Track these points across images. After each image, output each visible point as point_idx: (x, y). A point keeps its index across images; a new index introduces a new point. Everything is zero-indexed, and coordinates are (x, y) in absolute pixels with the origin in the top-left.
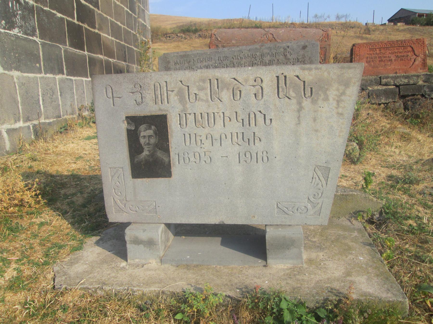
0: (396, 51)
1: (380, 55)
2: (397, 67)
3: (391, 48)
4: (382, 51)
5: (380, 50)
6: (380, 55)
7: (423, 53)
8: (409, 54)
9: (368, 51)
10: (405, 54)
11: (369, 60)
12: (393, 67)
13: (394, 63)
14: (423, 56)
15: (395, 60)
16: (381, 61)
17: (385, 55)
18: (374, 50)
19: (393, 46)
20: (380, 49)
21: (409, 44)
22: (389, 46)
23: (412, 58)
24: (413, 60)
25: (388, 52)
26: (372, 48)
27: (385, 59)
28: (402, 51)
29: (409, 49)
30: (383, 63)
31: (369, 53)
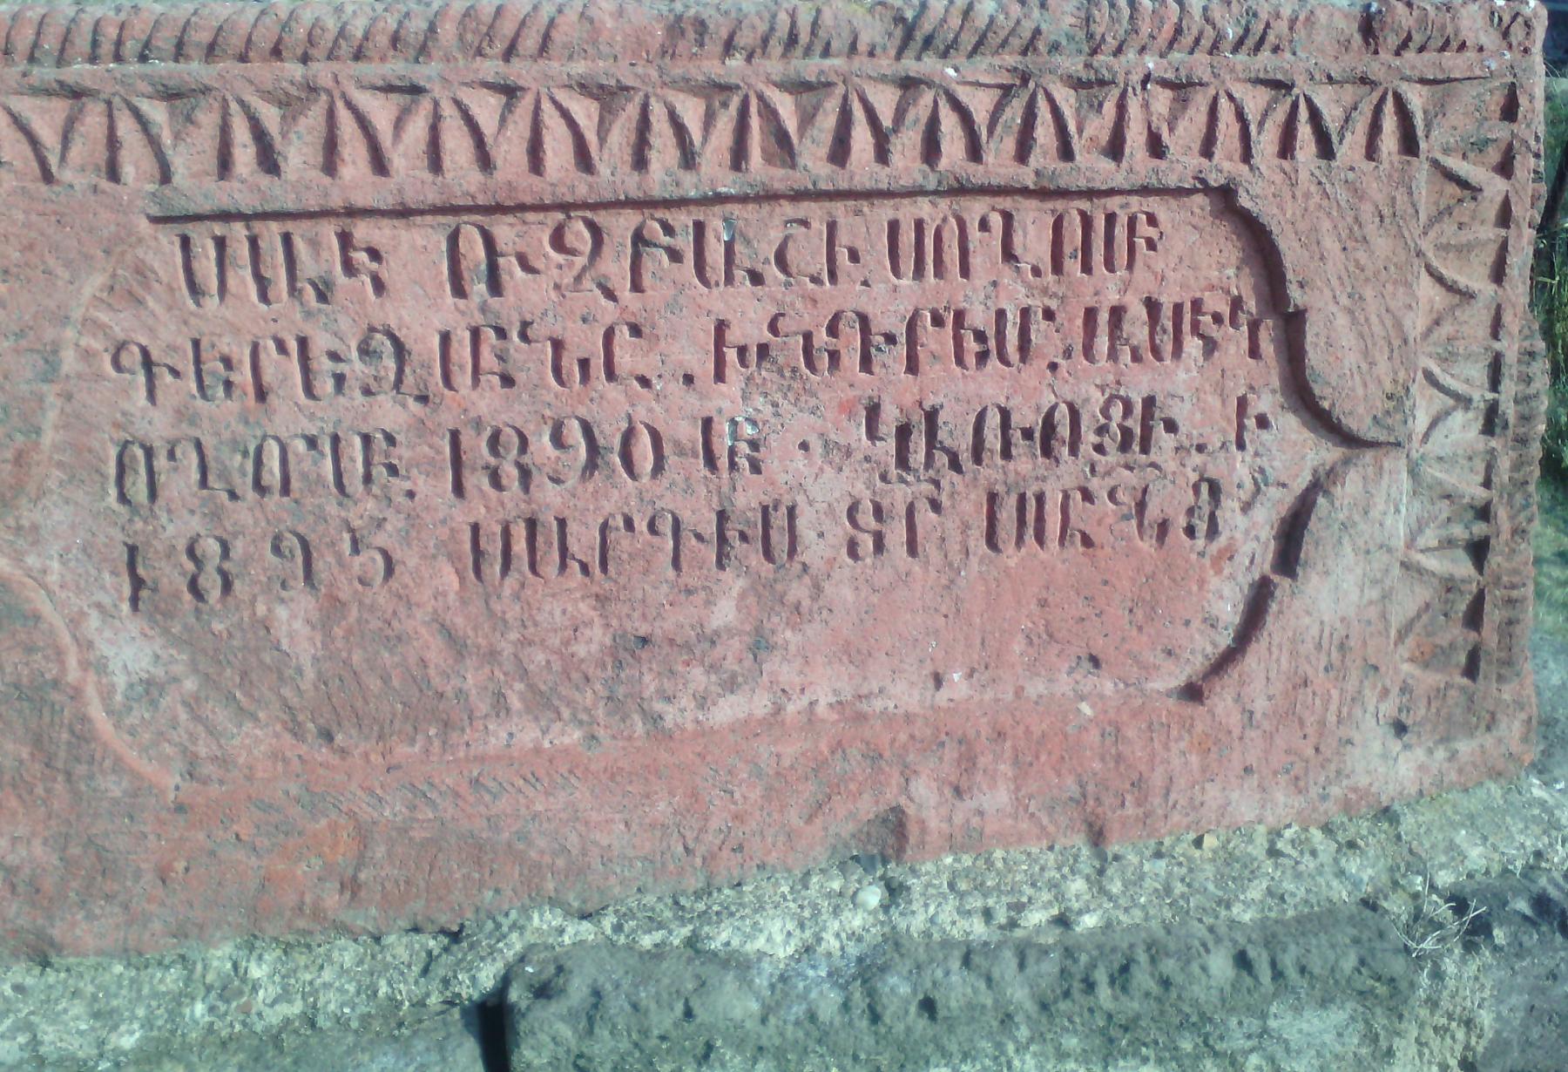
0: (891, 299)
1: (488, 402)
2: (905, 694)
3: (766, 230)
4: (526, 293)
5: (477, 273)
6: (488, 402)
7: (1470, 376)
8: (1187, 384)
9: (130, 290)
10: (1087, 386)
11: (180, 519)
12: (826, 689)
13: (841, 591)
14: (1463, 429)
15: (867, 530)
16: (535, 543)
17: (611, 407)
18: (319, 252)
19: (813, 160)
20: (475, 230)
21: (1184, 136)
22: (714, 170)
23: (1238, 470)
24: (1251, 533)
25: (685, 313)
26: (247, 186)
27: (619, 494)
28: (1015, 294)
29: (1194, 260)
30: (560, 602)
31: (166, 334)
